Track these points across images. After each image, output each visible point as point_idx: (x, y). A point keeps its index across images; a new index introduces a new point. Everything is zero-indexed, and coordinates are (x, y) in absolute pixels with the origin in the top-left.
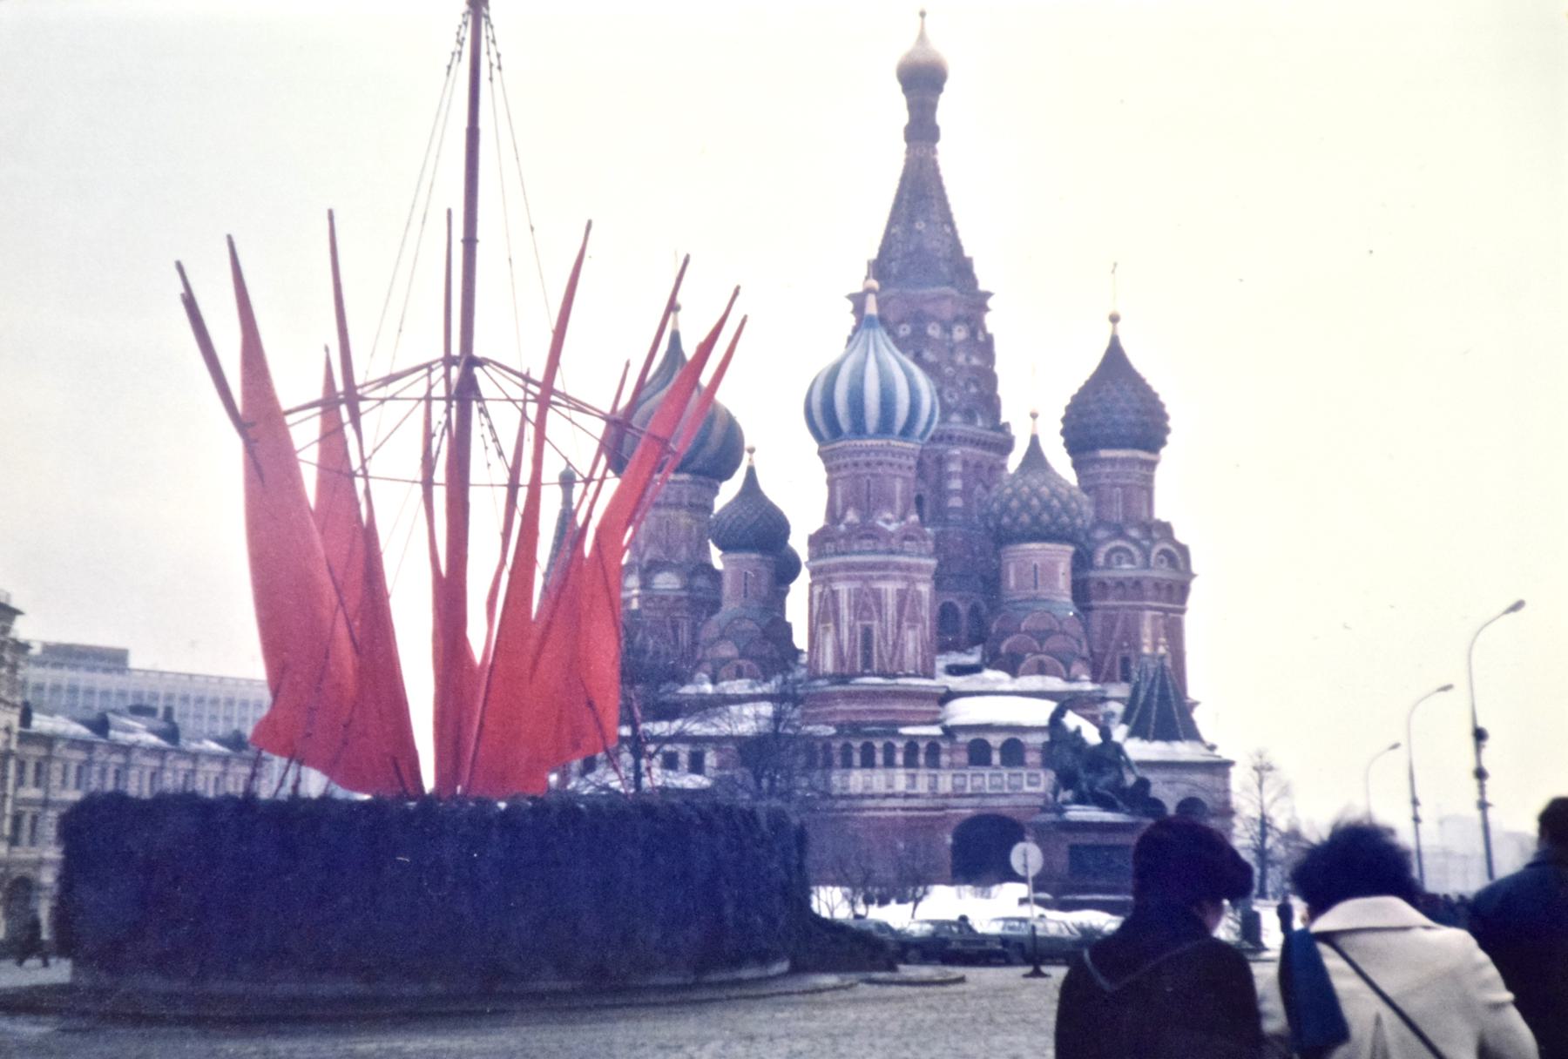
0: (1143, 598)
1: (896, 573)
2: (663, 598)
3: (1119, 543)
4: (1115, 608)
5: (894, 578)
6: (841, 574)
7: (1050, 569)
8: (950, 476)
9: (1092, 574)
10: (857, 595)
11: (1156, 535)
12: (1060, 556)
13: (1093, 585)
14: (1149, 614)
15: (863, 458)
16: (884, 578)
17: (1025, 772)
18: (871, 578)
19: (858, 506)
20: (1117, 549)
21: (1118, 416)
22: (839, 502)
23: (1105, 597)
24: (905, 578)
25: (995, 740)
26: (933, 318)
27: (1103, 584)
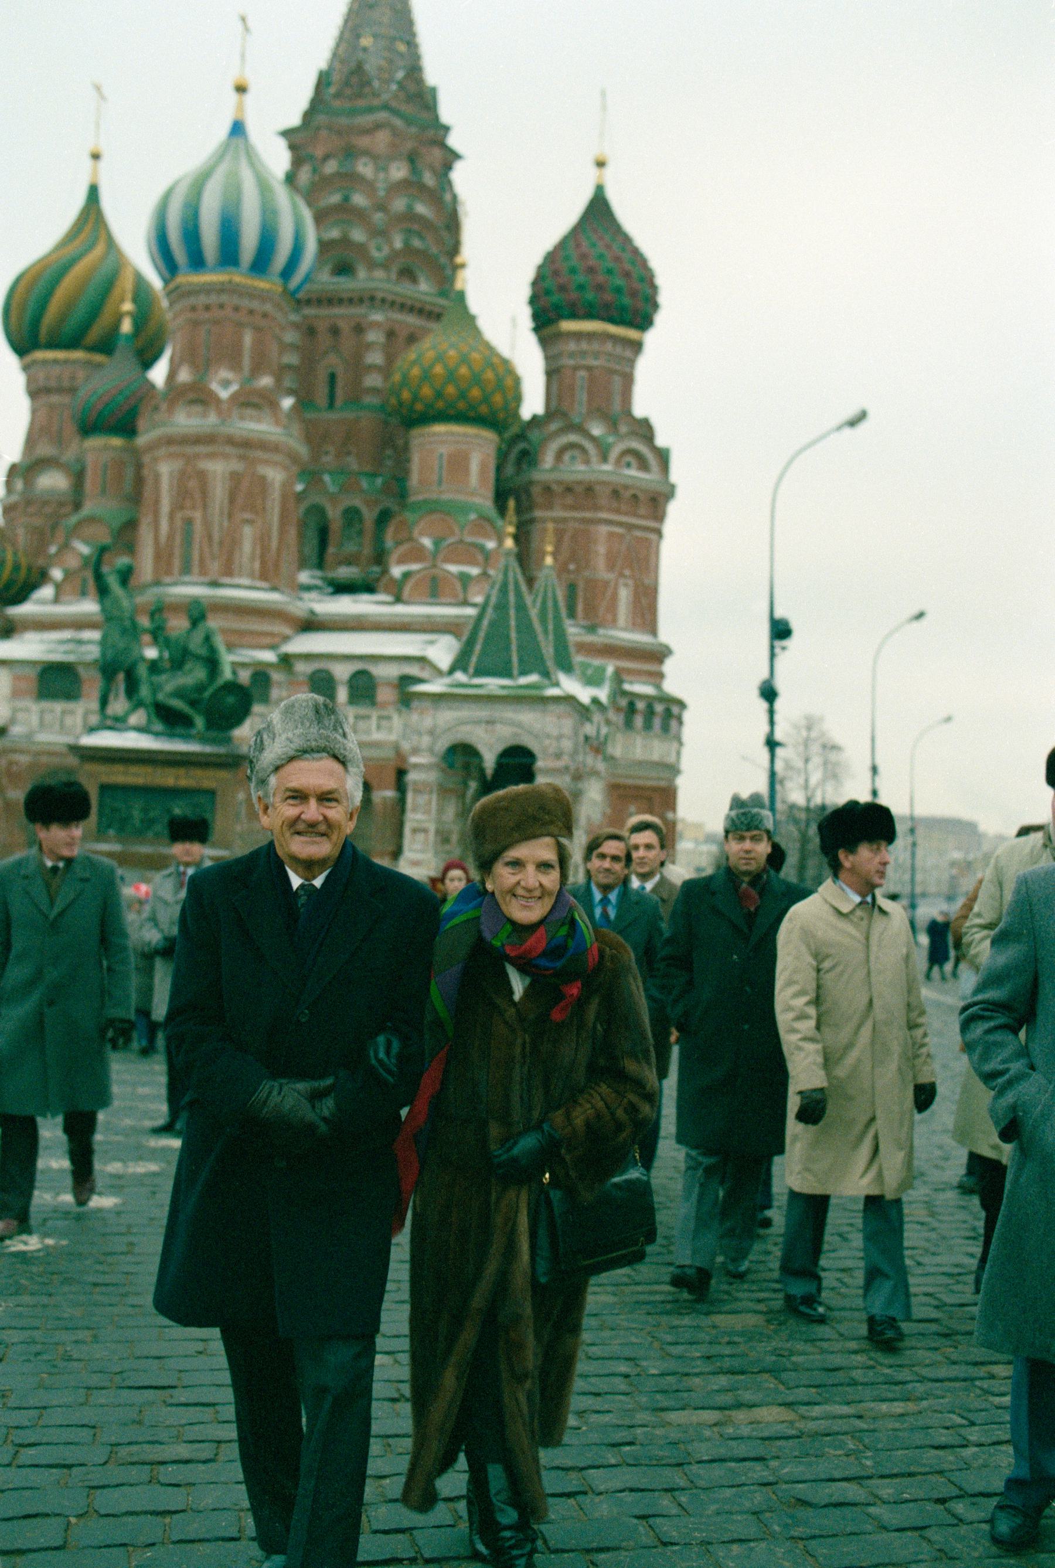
0: (596, 508)
1: (228, 449)
2: (45, 503)
3: (573, 438)
4: (565, 520)
5: (226, 457)
6: (162, 451)
7: (458, 463)
8: (369, 346)
9: (537, 476)
10: (182, 477)
11: (623, 429)
12: (479, 449)
13: (536, 490)
14: (604, 529)
15: (202, 300)
16: (211, 456)
17: (375, 714)
18: (197, 456)
19: (194, 365)
20: (572, 446)
21: (598, 288)
22: (177, 359)
23: (550, 506)
24: (242, 458)
25: (342, 672)
26: (366, 153)
27: (547, 489)
